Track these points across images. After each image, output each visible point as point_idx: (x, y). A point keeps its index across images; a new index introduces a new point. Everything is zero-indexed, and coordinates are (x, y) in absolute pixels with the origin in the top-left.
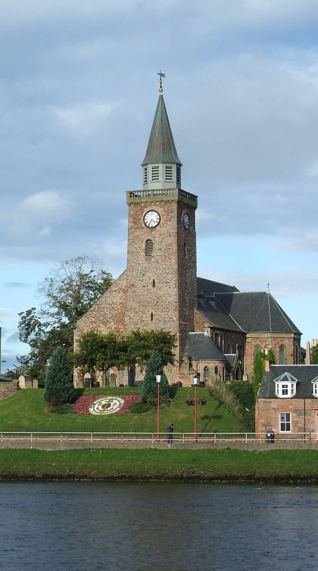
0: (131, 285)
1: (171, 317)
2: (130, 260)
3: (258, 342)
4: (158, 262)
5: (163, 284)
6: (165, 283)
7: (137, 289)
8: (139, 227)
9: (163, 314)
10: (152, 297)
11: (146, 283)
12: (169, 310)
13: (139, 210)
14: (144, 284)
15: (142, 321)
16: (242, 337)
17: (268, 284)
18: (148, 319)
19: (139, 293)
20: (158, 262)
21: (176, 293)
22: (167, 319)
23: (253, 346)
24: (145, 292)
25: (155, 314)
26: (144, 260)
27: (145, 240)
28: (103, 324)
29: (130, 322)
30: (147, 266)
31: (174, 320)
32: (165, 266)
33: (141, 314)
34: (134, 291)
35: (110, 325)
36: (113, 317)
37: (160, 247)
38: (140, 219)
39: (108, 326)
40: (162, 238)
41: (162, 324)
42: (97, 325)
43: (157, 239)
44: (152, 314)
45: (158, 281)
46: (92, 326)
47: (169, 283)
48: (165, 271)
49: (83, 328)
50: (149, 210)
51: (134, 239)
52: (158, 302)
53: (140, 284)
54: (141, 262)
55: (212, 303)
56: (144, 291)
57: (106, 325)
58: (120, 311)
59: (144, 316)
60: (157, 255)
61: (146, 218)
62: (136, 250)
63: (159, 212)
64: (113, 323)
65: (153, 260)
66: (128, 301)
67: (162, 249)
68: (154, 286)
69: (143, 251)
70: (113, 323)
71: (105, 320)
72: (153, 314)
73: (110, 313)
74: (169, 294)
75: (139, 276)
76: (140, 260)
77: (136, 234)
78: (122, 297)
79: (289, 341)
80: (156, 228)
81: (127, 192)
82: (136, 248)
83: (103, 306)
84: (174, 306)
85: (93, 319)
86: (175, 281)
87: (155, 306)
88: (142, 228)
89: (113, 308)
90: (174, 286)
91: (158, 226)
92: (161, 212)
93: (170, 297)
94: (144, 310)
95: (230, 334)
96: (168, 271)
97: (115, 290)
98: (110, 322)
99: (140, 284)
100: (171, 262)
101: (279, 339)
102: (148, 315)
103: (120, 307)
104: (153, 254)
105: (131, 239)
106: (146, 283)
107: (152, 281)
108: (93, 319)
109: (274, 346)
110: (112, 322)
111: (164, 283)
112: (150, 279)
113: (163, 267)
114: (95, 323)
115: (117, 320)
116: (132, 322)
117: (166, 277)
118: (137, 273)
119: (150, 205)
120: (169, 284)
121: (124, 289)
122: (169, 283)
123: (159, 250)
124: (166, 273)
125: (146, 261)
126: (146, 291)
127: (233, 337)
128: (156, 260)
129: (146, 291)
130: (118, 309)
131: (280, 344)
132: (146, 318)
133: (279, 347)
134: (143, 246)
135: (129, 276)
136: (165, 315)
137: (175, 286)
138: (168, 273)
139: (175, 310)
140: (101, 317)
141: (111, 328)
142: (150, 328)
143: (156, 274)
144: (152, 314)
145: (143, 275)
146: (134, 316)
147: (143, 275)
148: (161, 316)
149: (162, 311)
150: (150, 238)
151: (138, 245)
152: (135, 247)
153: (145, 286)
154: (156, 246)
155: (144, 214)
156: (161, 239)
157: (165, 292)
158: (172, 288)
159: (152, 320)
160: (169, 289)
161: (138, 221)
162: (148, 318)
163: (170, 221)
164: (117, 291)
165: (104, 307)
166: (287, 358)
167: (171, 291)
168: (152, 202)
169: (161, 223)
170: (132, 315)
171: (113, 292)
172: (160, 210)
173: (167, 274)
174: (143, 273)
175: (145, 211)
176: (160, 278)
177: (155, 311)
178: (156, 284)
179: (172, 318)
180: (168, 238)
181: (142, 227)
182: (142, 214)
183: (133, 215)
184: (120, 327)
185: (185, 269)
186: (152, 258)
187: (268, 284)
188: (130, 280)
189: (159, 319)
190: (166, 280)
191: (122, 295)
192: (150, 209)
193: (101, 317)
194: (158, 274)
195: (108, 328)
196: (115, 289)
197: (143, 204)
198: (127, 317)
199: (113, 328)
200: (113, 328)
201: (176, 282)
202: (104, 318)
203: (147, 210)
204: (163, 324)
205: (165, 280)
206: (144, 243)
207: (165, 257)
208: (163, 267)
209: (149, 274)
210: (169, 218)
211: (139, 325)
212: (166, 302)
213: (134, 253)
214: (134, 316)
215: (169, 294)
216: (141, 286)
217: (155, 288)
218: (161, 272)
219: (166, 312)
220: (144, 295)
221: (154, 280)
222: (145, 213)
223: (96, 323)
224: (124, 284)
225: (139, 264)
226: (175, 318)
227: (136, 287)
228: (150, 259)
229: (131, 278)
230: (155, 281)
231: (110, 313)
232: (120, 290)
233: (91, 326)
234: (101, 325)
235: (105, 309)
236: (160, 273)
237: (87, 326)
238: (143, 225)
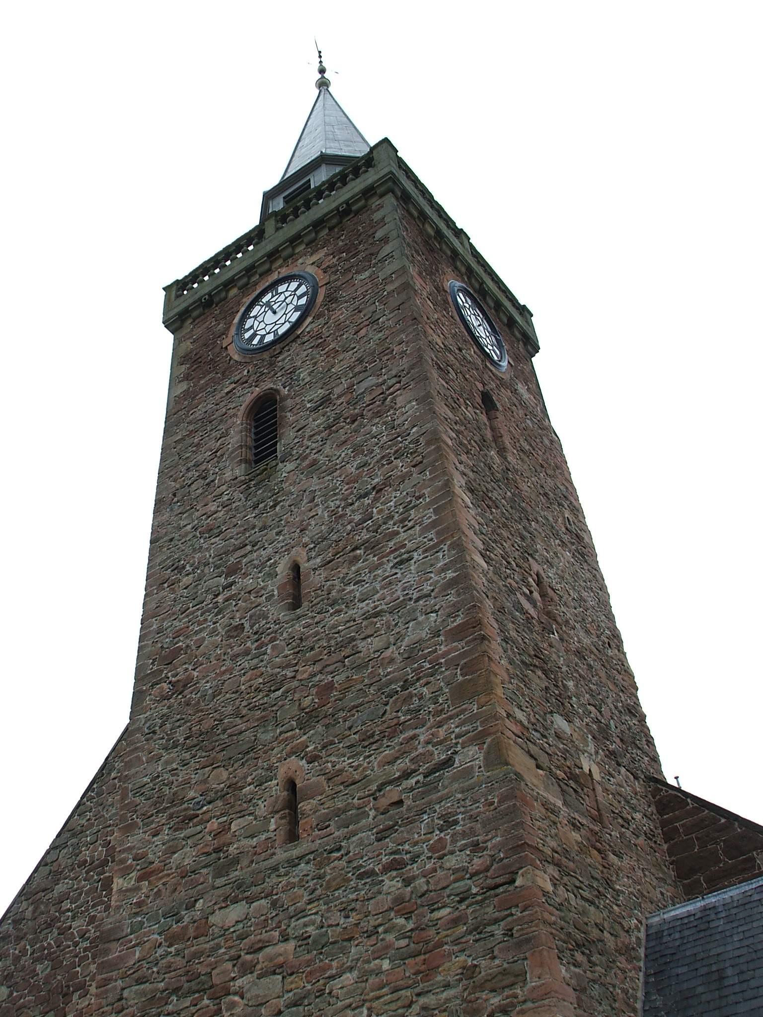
21: (450, 574)
31: (467, 773)
41: (369, 836)
44: (291, 785)
68: (296, 604)
81: (164, 289)
90: (432, 534)
99: (214, 632)
102: (262, 809)
112: (272, 575)
137: (437, 533)
140: (39, 967)
144: (291, 785)
170: (155, 851)
193: (39, 967)
198: (125, 872)
201: (436, 511)
202: (56, 965)
211: (199, 905)
221: (296, 568)
230: (305, 566)
235: (66, 905)
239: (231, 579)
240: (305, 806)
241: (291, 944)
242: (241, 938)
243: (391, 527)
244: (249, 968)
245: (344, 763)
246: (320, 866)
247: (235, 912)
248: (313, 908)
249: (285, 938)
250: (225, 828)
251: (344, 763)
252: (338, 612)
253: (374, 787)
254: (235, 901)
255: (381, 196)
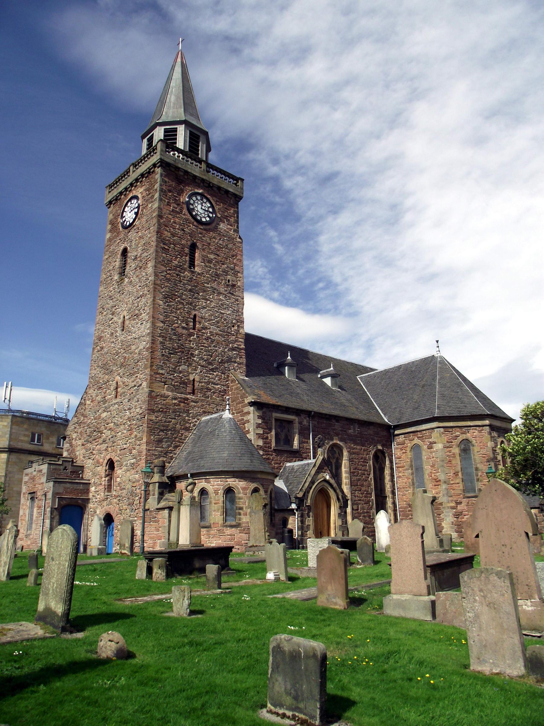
3: (416, 441)
16: (385, 433)
17: (437, 341)
23: (408, 449)
55: (328, 381)
79: (480, 432)
95: (337, 426)
101: (458, 429)
109: (448, 445)
127: (351, 431)
131: (460, 439)
133: (459, 446)
139: (145, 368)
166: (478, 466)
185: (190, 290)
187: (437, 341)
226: (145, 384)
255: (158, 168)
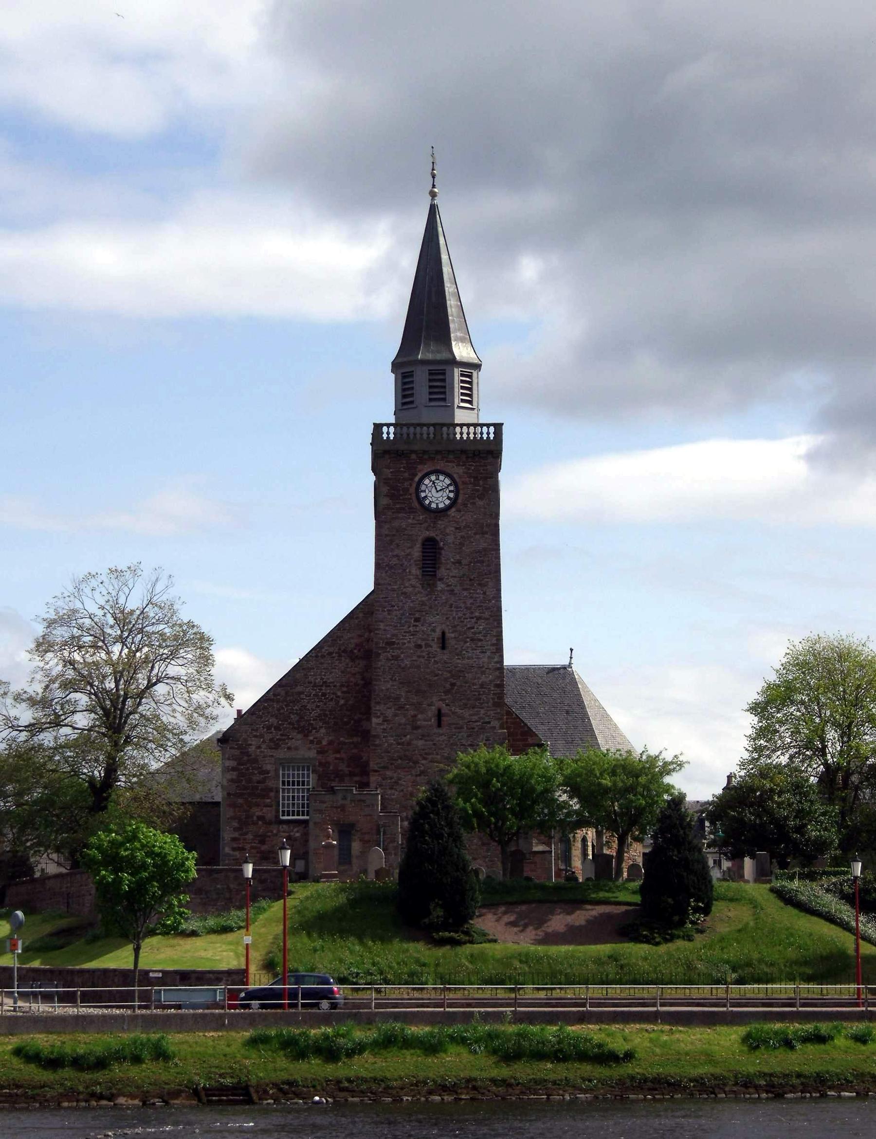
0: (387, 643)
1: (487, 720)
2: (384, 584)
4: (453, 590)
5: (466, 642)
6: (471, 640)
7: (402, 653)
8: (403, 509)
9: (466, 713)
10: (440, 672)
11: (423, 640)
12: (482, 704)
13: (404, 467)
14: (419, 642)
15: (417, 728)
18: (430, 723)
19: (407, 662)
20: (453, 590)
22: (479, 724)
24: (422, 660)
25: (447, 711)
26: (418, 585)
27: (420, 539)
28: (298, 733)
29: (384, 729)
30: (424, 599)
31: (494, 728)
32: (471, 601)
33: (412, 713)
34: (392, 656)
35: (318, 735)
36: (326, 715)
37: (458, 557)
38: (406, 490)
39: (311, 738)
40: (462, 537)
42: (282, 735)
43: (450, 539)
44: (439, 711)
45: (453, 635)
46: (270, 736)
47: (481, 640)
48: (472, 613)
49: (245, 740)
50: (429, 470)
51: (394, 535)
52: (453, 685)
53: (409, 642)
54: (410, 589)
56: (419, 657)
57: (306, 736)
58: (342, 702)
59: (419, 716)
60: (451, 574)
61: (423, 487)
62: (397, 562)
63: (455, 476)
64: (323, 731)
65: (440, 586)
66: (380, 679)
67: (464, 562)
68: (443, 647)
69: (416, 565)
70: (323, 731)
71: (302, 724)
72: (443, 712)
73: (318, 707)
74: (483, 667)
75: (406, 622)
76: (407, 585)
77: (396, 524)
78: (348, 670)
80: (449, 513)
82: (397, 556)
83: (299, 689)
84: (494, 694)
85: (273, 721)
86: (495, 636)
87: (447, 692)
88: (412, 510)
89: (324, 695)
90: (494, 647)
91: (453, 509)
92: (460, 477)
93: (483, 673)
94: (420, 704)
96: (477, 614)
97: (330, 654)
98: (315, 729)
99: (409, 642)
100: (484, 593)
102: (430, 714)
103: (343, 692)
104: (442, 572)
105: (387, 535)
106: (423, 640)
107: (438, 633)
108: (273, 721)
110: (322, 727)
111: (468, 640)
112: (434, 631)
113: (465, 603)
114: (277, 728)
115: (336, 724)
116: (391, 728)
117: (473, 628)
118: (403, 614)
119: (433, 459)
120: (480, 644)
121: (351, 651)
122: (481, 640)
123: (453, 563)
124: (473, 618)
125: (423, 587)
126: (424, 657)
128: (448, 586)
129: (424, 657)
130: (338, 697)
132: (425, 720)
134: (416, 552)
135: (382, 622)
136: (471, 715)
138: (478, 618)
140: (292, 716)
141: (319, 742)
142: (434, 744)
143: (447, 618)
144: (439, 711)
145: (417, 620)
146: (396, 715)
147: (417, 620)
148: (463, 718)
149: (466, 705)
150: (432, 534)
151: (403, 551)
152: (395, 553)
153: (420, 646)
154: (448, 555)
155: (417, 479)
156: (459, 537)
157: (471, 662)
158: (488, 653)
159: (439, 725)
160: (482, 655)
161: (402, 495)
162: (430, 720)
163: (481, 498)
164: (334, 655)
165: (302, 693)
167: (486, 660)
168: (438, 452)
169: (460, 501)
170: (390, 713)
171: (323, 656)
172: (458, 471)
173: (474, 620)
174: (417, 615)
175: (420, 471)
176: (459, 628)
177: (447, 705)
178: (451, 643)
179: (489, 723)
180: (478, 536)
181: (413, 508)
182: (412, 479)
183: (390, 479)
184: (342, 739)
186: (439, 583)
188: (385, 630)
189: (457, 724)
190: (475, 633)
191: (347, 664)
192: (433, 468)
193: (292, 716)
194: (454, 618)
195: (312, 742)
196: (331, 650)
197: (414, 456)
198: (379, 717)
199: (324, 743)
200: (324, 743)
203: (426, 468)
204: (468, 736)
205: (470, 635)
206: (418, 547)
207: (471, 580)
208: (465, 603)
209: (430, 619)
210: (478, 490)
211: (408, 736)
212: (474, 684)
213: (391, 568)
214: (396, 715)
215: (483, 667)
216: (412, 645)
217: (445, 651)
218: (460, 615)
219: (473, 708)
220: (418, 667)
221: (443, 633)
222: (420, 475)
223: (280, 730)
224: (352, 641)
225: (405, 593)
227: (399, 649)
228: (434, 585)
229: (387, 626)
230: (448, 635)
231: (318, 707)
232: (343, 654)
233: (268, 737)
234: (294, 734)
235: (302, 696)
236: (459, 618)
237: (256, 736)
238: (416, 504)
239: (417, 624)
240: (444, 719)
241: (439, 757)
242: (423, 750)
243: (480, 637)
244: (425, 759)
245: (458, 710)
246: (449, 738)
247: (420, 743)
248: (446, 749)
249: (437, 754)
250: (415, 716)
251: (458, 710)
252: (459, 659)
253: (466, 721)
254: (421, 739)
